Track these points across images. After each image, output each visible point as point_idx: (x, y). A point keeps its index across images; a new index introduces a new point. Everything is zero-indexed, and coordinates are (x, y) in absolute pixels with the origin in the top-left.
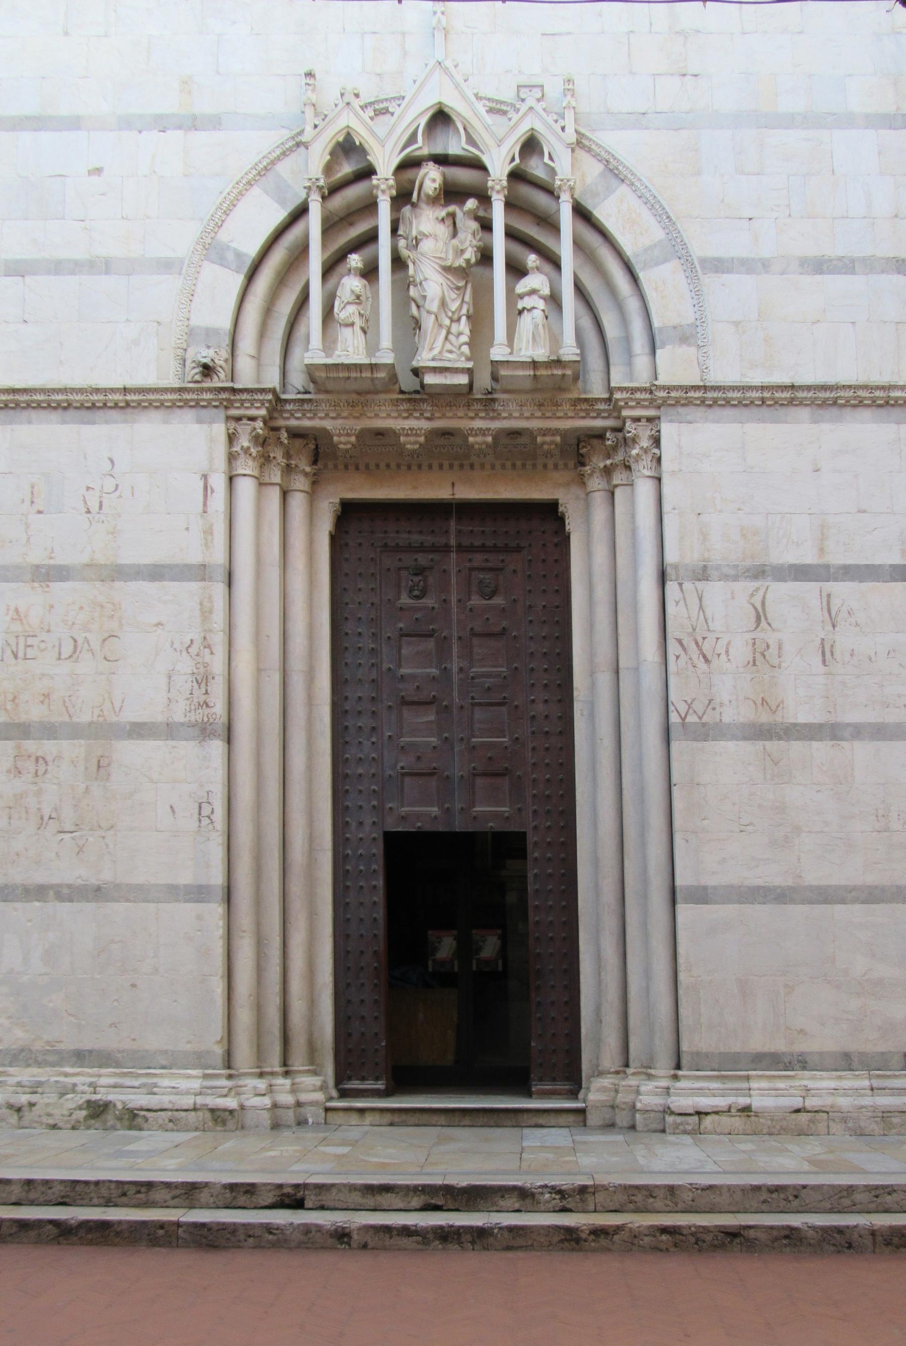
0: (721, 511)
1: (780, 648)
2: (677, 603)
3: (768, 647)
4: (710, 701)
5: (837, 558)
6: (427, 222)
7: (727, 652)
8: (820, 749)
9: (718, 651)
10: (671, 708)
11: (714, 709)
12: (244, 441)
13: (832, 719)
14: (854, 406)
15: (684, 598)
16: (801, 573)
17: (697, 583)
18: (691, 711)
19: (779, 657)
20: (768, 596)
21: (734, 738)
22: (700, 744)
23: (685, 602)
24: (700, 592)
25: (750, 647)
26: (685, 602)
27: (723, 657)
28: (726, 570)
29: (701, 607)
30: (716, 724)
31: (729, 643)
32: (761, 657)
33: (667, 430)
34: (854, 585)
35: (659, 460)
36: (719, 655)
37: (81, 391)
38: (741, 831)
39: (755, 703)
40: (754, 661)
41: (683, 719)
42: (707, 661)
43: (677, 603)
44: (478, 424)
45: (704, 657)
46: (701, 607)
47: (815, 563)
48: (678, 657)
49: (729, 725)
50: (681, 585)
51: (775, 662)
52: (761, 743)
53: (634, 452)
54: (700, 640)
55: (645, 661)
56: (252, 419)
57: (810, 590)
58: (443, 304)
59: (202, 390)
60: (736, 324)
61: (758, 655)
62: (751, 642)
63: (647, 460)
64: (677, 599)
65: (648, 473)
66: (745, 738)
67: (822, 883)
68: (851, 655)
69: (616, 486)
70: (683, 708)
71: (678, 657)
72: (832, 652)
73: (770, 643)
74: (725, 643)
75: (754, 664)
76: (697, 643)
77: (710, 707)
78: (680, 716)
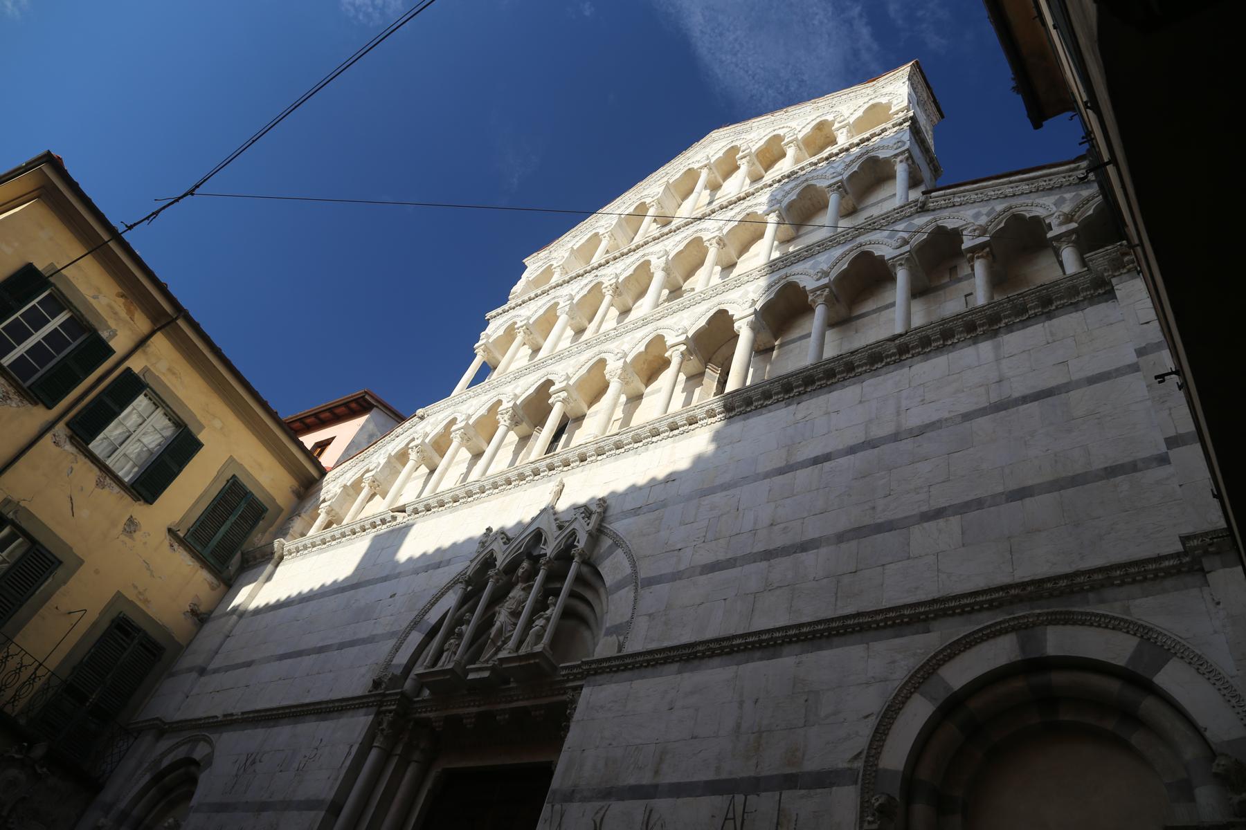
6: (516, 593)
12: (384, 726)
14: (710, 657)
33: (585, 690)
37: (327, 702)
44: (502, 706)
56: (390, 712)
57: (637, 808)
58: (500, 631)
59: (374, 696)
60: (650, 615)
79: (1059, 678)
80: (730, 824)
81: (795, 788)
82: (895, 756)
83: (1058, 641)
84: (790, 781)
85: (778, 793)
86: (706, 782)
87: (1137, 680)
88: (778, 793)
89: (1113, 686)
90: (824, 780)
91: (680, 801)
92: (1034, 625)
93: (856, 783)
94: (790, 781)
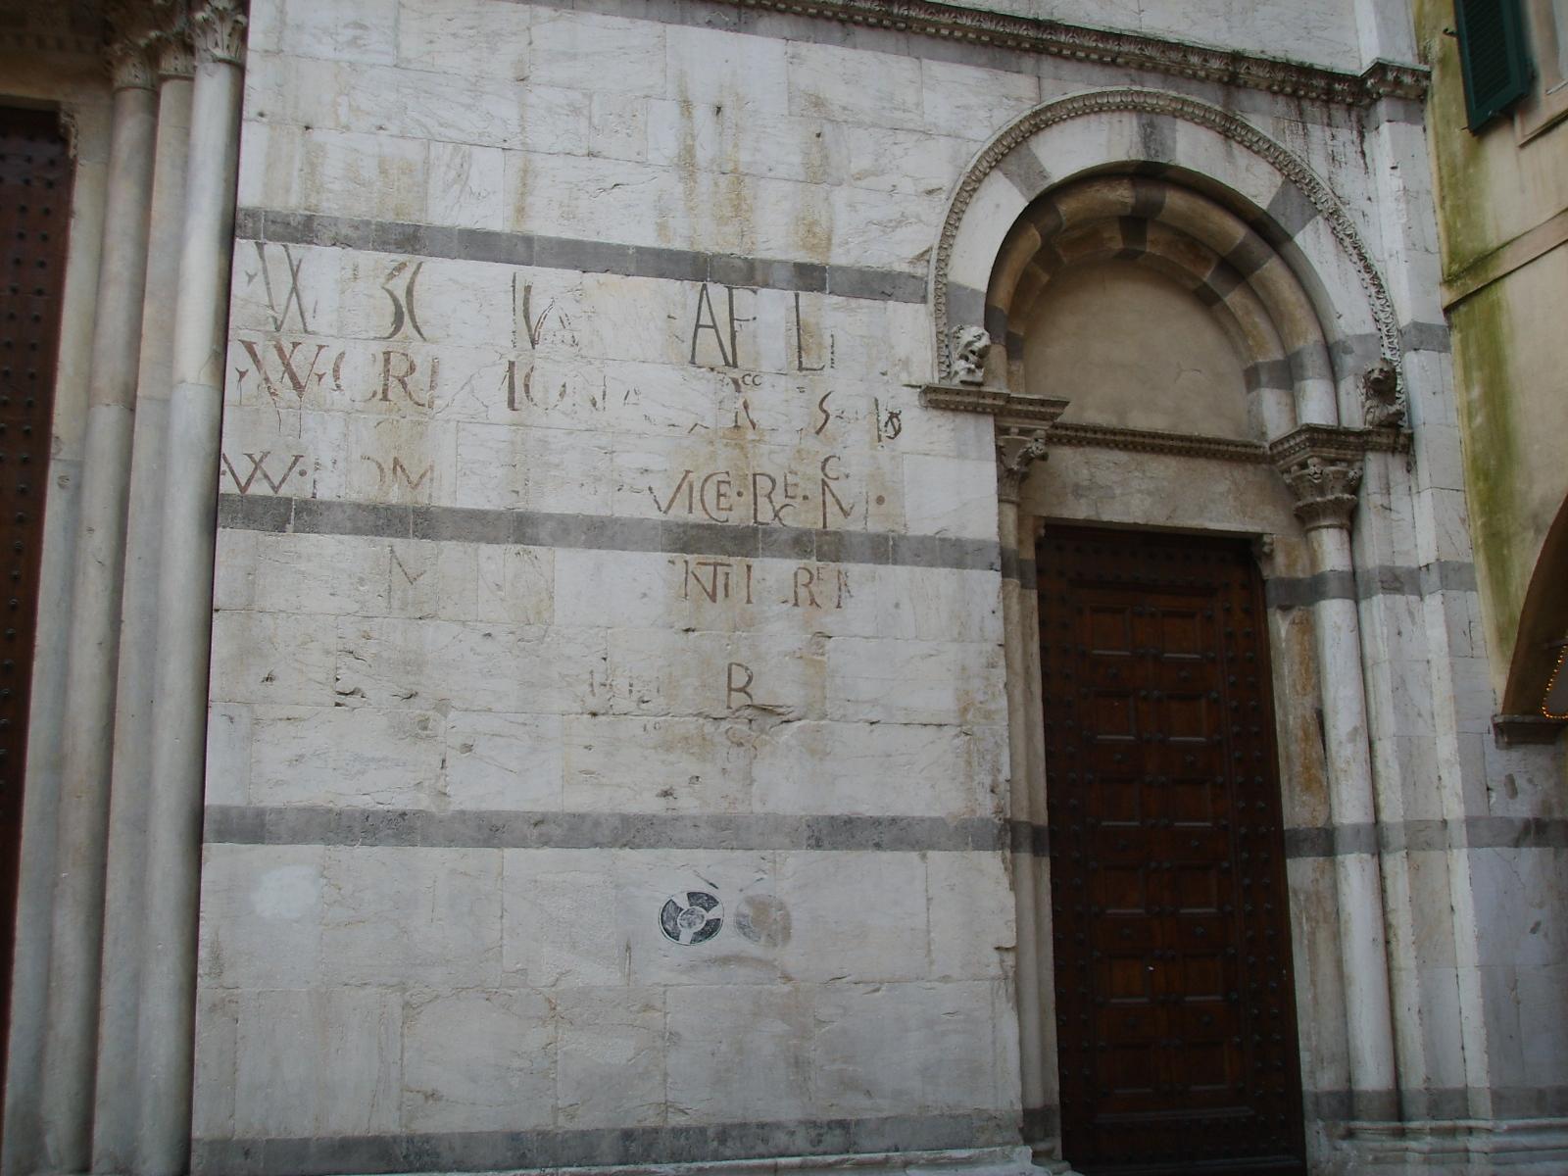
0: (347, 128)
1: (434, 372)
2: (251, 278)
3: (412, 368)
4: (297, 458)
5: (545, 225)
7: (336, 371)
8: (497, 559)
9: (319, 369)
10: (224, 467)
11: (303, 473)
13: (521, 506)
15: (265, 270)
16: (479, 245)
17: (290, 245)
18: (259, 474)
19: (432, 388)
20: (419, 278)
21: (337, 529)
22: (271, 538)
23: (266, 277)
24: (295, 263)
25: (380, 366)
26: (266, 277)
27: (329, 380)
28: (345, 231)
29: (295, 289)
30: (306, 502)
31: (342, 355)
32: (400, 384)
34: (573, 275)
35: (242, 34)
36: (320, 377)
38: (338, 705)
39: (382, 470)
40: (385, 392)
41: (243, 489)
42: (298, 387)
43: (251, 278)
45: (293, 377)
46: (295, 289)
47: (507, 230)
48: (242, 374)
49: (329, 505)
50: (260, 246)
51: (424, 397)
52: (387, 541)
53: (199, 16)
54: (287, 348)
55: (183, 381)
57: (496, 274)
61: (393, 383)
62: (381, 357)
63: (223, 31)
64: (251, 273)
65: (219, 53)
66: (356, 531)
67: (484, 807)
68: (562, 395)
69: (164, 79)
70: (243, 468)
71: (242, 374)
72: (527, 386)
73: (418, 361)
74: (334, 354)
75: (385, 398)
76: (280, 350)
77: (297, 469)
78: (238, 483)
79: (1175, 201)
80: (707, 337)
81: (821, 289)
82: (974, 265)
83: (1193, 148)
84: (810, 277)
85: (791, 294)
86: (640, 250)
87: (1269, 232)
88: (791, 294)
89: (1238, 232)
90: (875, 285)
91: (590, 279)
92: (1163, 112)
93: (924, 300)
94: (810, 277)
